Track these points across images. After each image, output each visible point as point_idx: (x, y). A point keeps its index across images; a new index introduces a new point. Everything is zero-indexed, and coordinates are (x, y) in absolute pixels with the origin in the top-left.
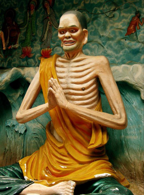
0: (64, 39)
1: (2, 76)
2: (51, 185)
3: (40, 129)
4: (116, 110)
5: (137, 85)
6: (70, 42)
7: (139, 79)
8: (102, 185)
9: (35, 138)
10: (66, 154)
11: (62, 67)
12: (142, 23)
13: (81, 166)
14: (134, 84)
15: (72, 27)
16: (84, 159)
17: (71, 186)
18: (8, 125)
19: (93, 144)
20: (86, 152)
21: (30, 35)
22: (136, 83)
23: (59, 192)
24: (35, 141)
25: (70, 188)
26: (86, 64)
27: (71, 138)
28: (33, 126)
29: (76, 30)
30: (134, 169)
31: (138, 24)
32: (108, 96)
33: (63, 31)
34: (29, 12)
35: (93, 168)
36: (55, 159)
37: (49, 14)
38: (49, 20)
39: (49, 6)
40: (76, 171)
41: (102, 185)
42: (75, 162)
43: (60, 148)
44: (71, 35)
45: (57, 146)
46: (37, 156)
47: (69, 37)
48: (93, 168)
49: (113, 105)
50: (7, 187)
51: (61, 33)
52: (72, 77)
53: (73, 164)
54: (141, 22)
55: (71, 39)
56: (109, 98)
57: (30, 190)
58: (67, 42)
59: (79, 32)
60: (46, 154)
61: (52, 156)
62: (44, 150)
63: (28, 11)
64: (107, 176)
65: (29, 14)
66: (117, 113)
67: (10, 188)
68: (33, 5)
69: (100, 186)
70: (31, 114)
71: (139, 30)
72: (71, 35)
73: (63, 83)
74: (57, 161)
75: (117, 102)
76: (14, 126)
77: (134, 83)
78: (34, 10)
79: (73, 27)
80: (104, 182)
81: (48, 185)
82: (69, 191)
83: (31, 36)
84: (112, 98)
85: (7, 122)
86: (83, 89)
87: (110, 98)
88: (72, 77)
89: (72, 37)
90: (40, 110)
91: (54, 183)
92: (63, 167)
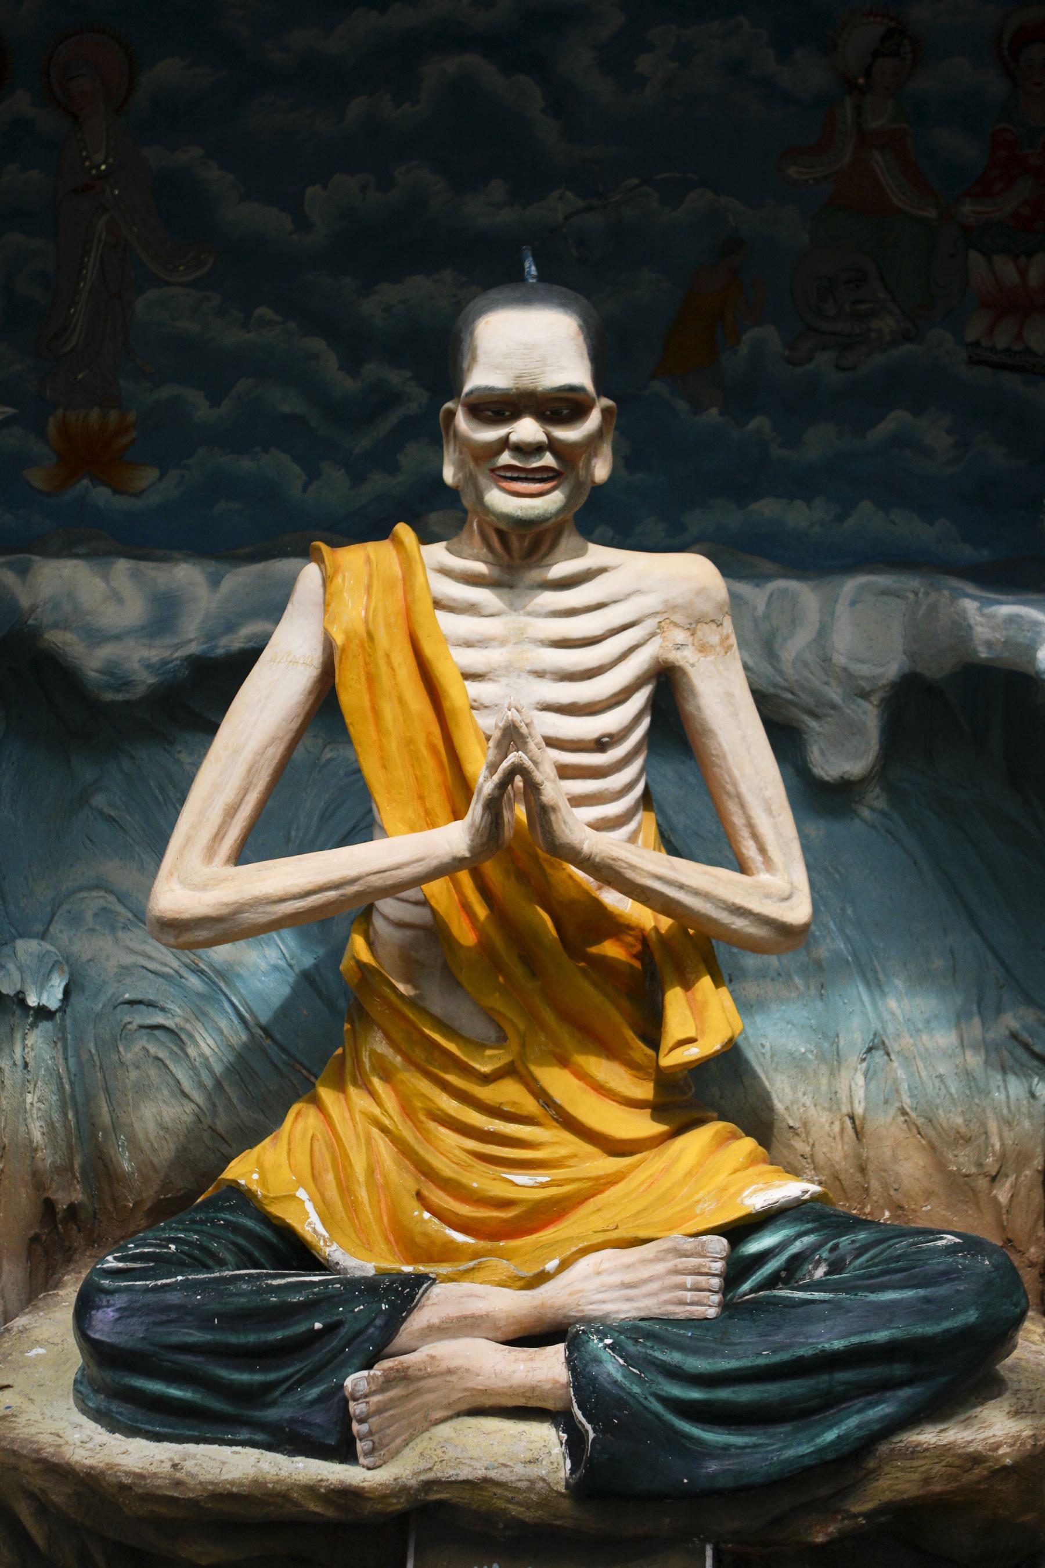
0: (499, 452)
2: (542, 1278)
3: (167, 970)
4: (762, 850)
5: (789, 696)
7: (806, 665)
8: (808, 1240)
9: (144, 1031)
10: (530, 1105)
11: (471, 609)
14: (772, 690)
15: (565, 395)
16: (640, 1125)
17: (705, 1257)
19: (691, 1041)
20: (645, 1091)
22: (786, 689)
23: (591, 1307)
24: (144, 1049)
25: (706, 1270)
26: (615, 602)
27: (549, 1016)
28: (107, 958)
30: (809, 1160)
32: (727, 777)
40: (601, 1192)
41: (808, 1240)
43: (487, 1079)
45: (466, 1070)
47: (537, 449)
49: (751, 826)
50: (318, 1325)
52: (540, 674)
53: (575, 1156)
55: (548, 460)
56: (730, 787)
57: (435, 1321)
59: (593, 420)
60: (387, 1122)
61: (432, 1125)
64: (807, 1196)
67: (331, 1329)
69: (797, 1247)
72: (548, 435)
73: (486, 707)
75: (769, 811)
79: (571, 395)
80: (810, 1226)
81: (521, 1283)
82: (704, 1285)
86: (600, 745)
87: (735, 785)
88: (540, 674)
89: (552, 446)
90: (393, 872)
91: (551, 1265)
92: (521, 1178)
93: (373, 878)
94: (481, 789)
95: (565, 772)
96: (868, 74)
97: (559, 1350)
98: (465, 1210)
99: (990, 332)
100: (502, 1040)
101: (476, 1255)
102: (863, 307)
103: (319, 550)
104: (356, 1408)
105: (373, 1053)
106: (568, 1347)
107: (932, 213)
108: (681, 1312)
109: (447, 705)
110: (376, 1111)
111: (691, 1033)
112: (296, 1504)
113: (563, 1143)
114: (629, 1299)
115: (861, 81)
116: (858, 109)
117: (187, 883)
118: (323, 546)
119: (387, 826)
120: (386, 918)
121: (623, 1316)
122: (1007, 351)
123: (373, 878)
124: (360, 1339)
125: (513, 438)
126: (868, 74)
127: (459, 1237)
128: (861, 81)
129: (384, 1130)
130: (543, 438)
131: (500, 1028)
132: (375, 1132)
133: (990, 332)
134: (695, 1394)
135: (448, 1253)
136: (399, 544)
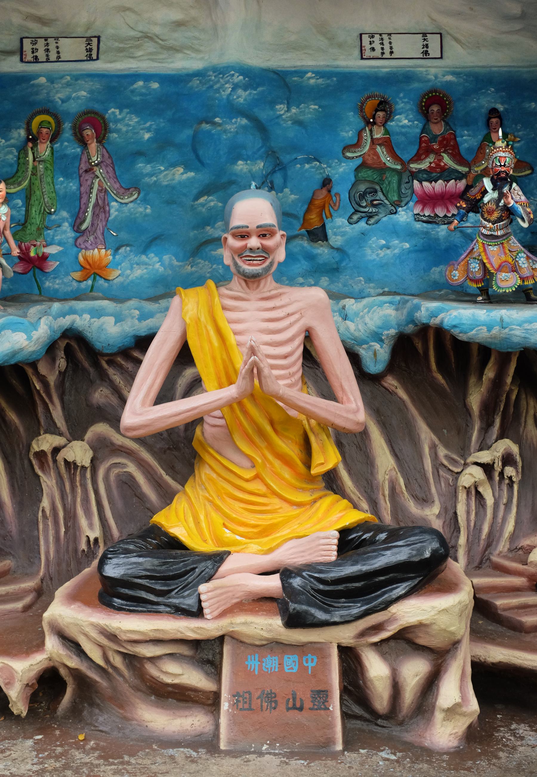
1: (39, 329)
6: (258, 259)
12: (335, 205)
13: (298, 511)
18: (41, 449)
19: (322, 464)
21: (40, 211)
27: (270, 457)
29: (272, 234)
31: (326, 206)
33: (244, 235)
34: (32, 149)
35: (328, 510)
36: (238, 505)
37: (94, 159)
38: (98, 177)
39: (95, 140)
42: (285, 505)
43: (247, 481)
44: (261, 244)
45: (240, 477)
46: (186, 505)
48: (328, 510)
49: (341, 386)
51: (235, 236)
54: (335, 202)
58: (253, 259)
59: (278, 237)
61: (228, 499)
62: (202, 489)
63: (30, 145)
65: (33, 153)
66: (349, 399)
68: (48, 130)
70: (180, 414)
71: (330, 219)
72: (261, 244)
73: (243, 344)
74: (242, 508)
76: (56, 450)
77: (348, 338)
78: (48, 142)
83: (43, 213)
84: (338, 373)
85: (38, 440)
86: (285, 357)
93: (203, 407)
94: (241, 373)
95: (273, 367)
96: (374, 118)
97: (277, 576)
98: (242, 529)
99: (423, 210)
100: (254, 466)
101: (245, 544)
102: (375, 202)
103: (180, 290)
104: (203, 597)
105: (205, 474)
106: (280, 575)
107: (399, 167)
108: (321, 559)
109: (228, 343)
110: (207, 495)
111: (323, 461)
112: (181, 633)
113: (276, 502)
114: (302, 557)
115: (371, 120)
116: (371, 131)
117: (135, 413)
118: (181, 290)
119: (208, 389)
120: (209, 424)
121: (301, 563)
122: (429, 216)
123: (203, 407)
124: (203, 573)
125: (249, 246)
126: (374, 118)
127: (238, 538)
128: (371, 120)
129: (211, 502)
130: (259, 245)
131: (252, 462)
132: (207, 504)
133: (423, 210)
134: (327, 588)
135: (235, 543)
136: (208, 288)
